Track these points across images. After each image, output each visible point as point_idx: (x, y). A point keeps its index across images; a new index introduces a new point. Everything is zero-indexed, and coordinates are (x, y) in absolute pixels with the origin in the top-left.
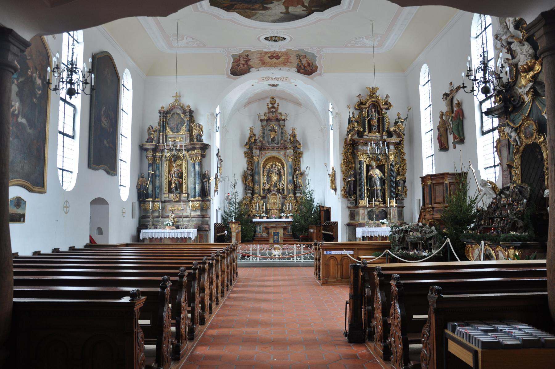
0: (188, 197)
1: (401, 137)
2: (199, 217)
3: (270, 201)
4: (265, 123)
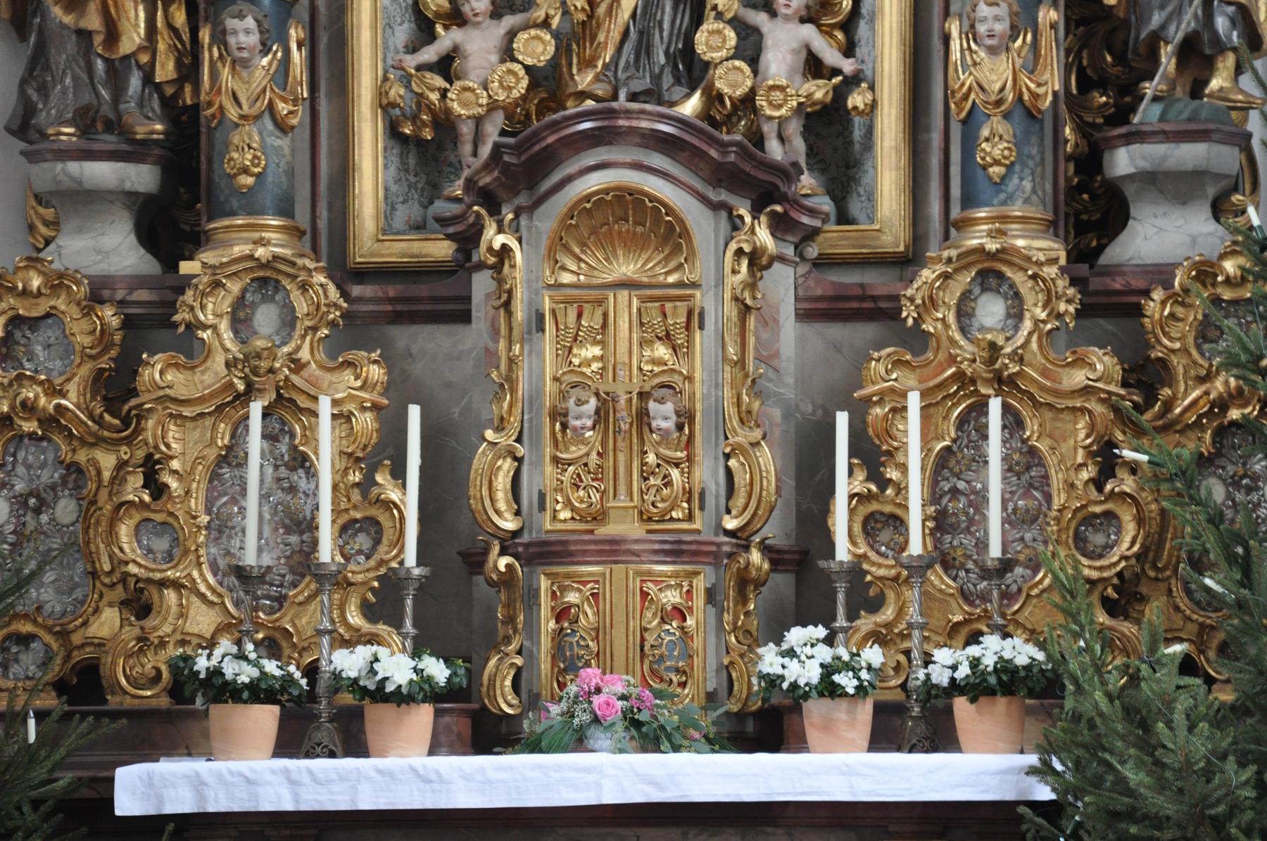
3: (541, 365)
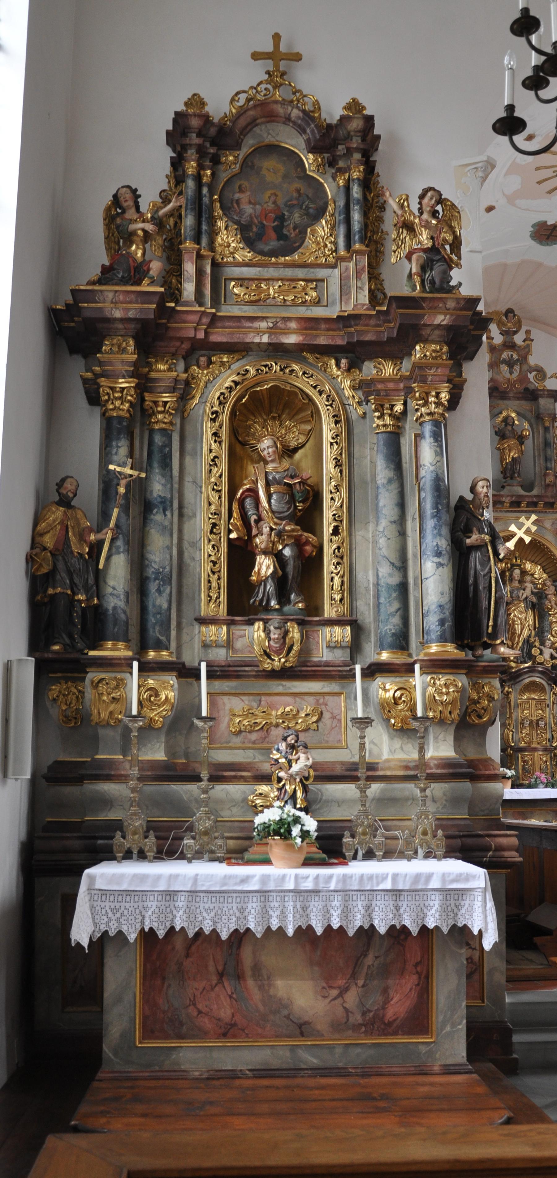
0: (355, 647)
3: (518, 714)
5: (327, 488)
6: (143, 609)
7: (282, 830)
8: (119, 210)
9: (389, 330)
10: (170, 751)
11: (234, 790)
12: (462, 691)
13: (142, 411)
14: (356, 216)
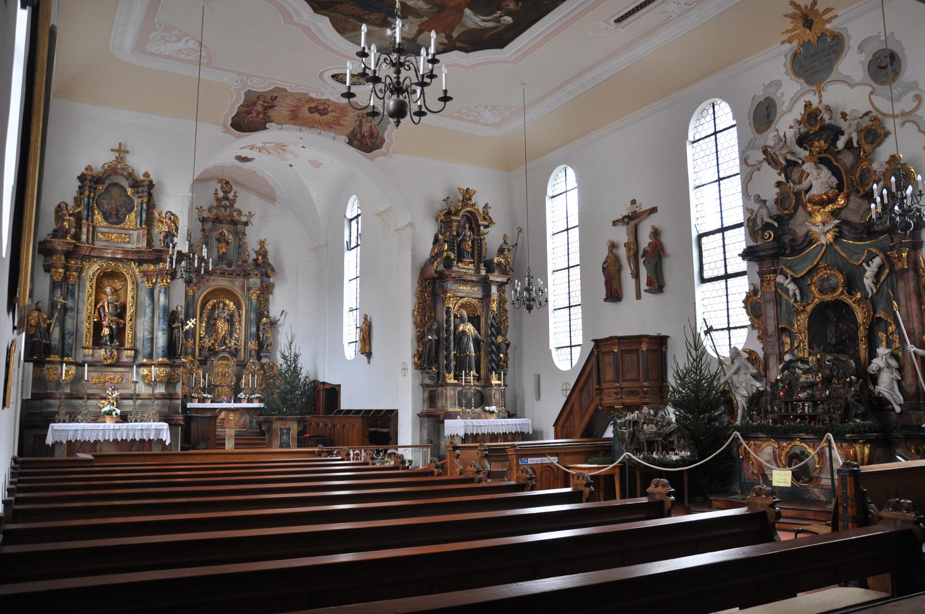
0: (135, 357)
1: (515, 273)
2: (163, 397)
3: (216, 370)
4: (209, 225)
5: (129, 305)
6: (63, 344)
7: (109, 413)
8: (60, 210)
9: (153, 256)
10: (71, 390)
11: (93, 402)
12: (168, 373)
13: (66, 278)
14: (144, 215)
